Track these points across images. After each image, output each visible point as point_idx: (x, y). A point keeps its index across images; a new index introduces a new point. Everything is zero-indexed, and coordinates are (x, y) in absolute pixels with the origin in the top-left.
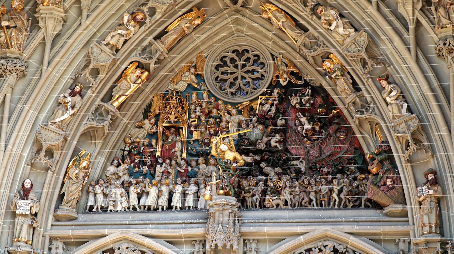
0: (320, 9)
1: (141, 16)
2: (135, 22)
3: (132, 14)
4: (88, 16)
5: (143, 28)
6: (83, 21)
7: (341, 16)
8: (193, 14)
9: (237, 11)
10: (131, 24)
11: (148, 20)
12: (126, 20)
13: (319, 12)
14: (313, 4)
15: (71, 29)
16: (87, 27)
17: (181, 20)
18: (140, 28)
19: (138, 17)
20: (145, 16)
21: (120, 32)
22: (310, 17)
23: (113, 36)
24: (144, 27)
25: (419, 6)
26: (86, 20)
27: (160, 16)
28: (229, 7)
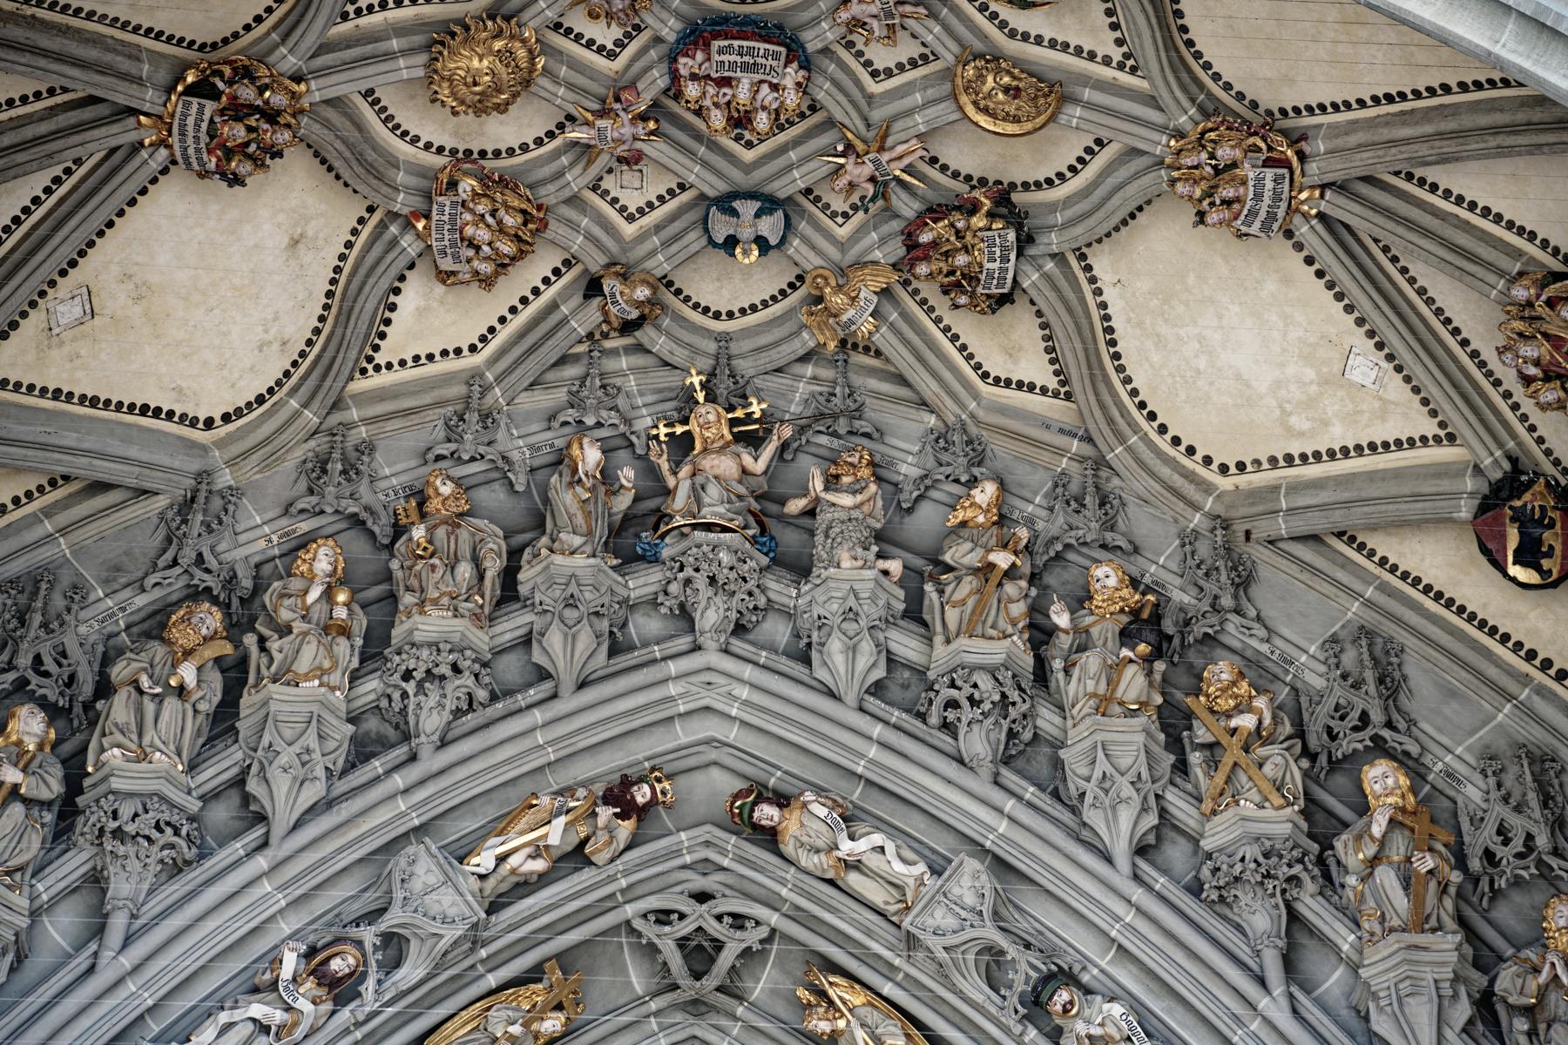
0: (1063, 996)
1: (351, 961)
2: (319, 985)
3: (312, 952)
4: (127, 942)
5: (345, 1015)
6: (107, 954)
7: (1148, 1035)
8: (537, 993)
9: (697, 1007)
10: (301, 990)
11: (370, 984)
12: (287, 971)
13: (1059, 1008)
14: (1034, 975)
15: (46, 986)
16: (120, 982)
17: (488, 1009)
18: (333, 1013)
19: (337, 965)
20: (365, 963)
21: (257, 1010)
22: (1018, 1029)
23: (229, 1026)
24: (352, 1011)
25: (1463, 1011)
26: (119, 952)
27: (420, 973)
28: (675, 987)
